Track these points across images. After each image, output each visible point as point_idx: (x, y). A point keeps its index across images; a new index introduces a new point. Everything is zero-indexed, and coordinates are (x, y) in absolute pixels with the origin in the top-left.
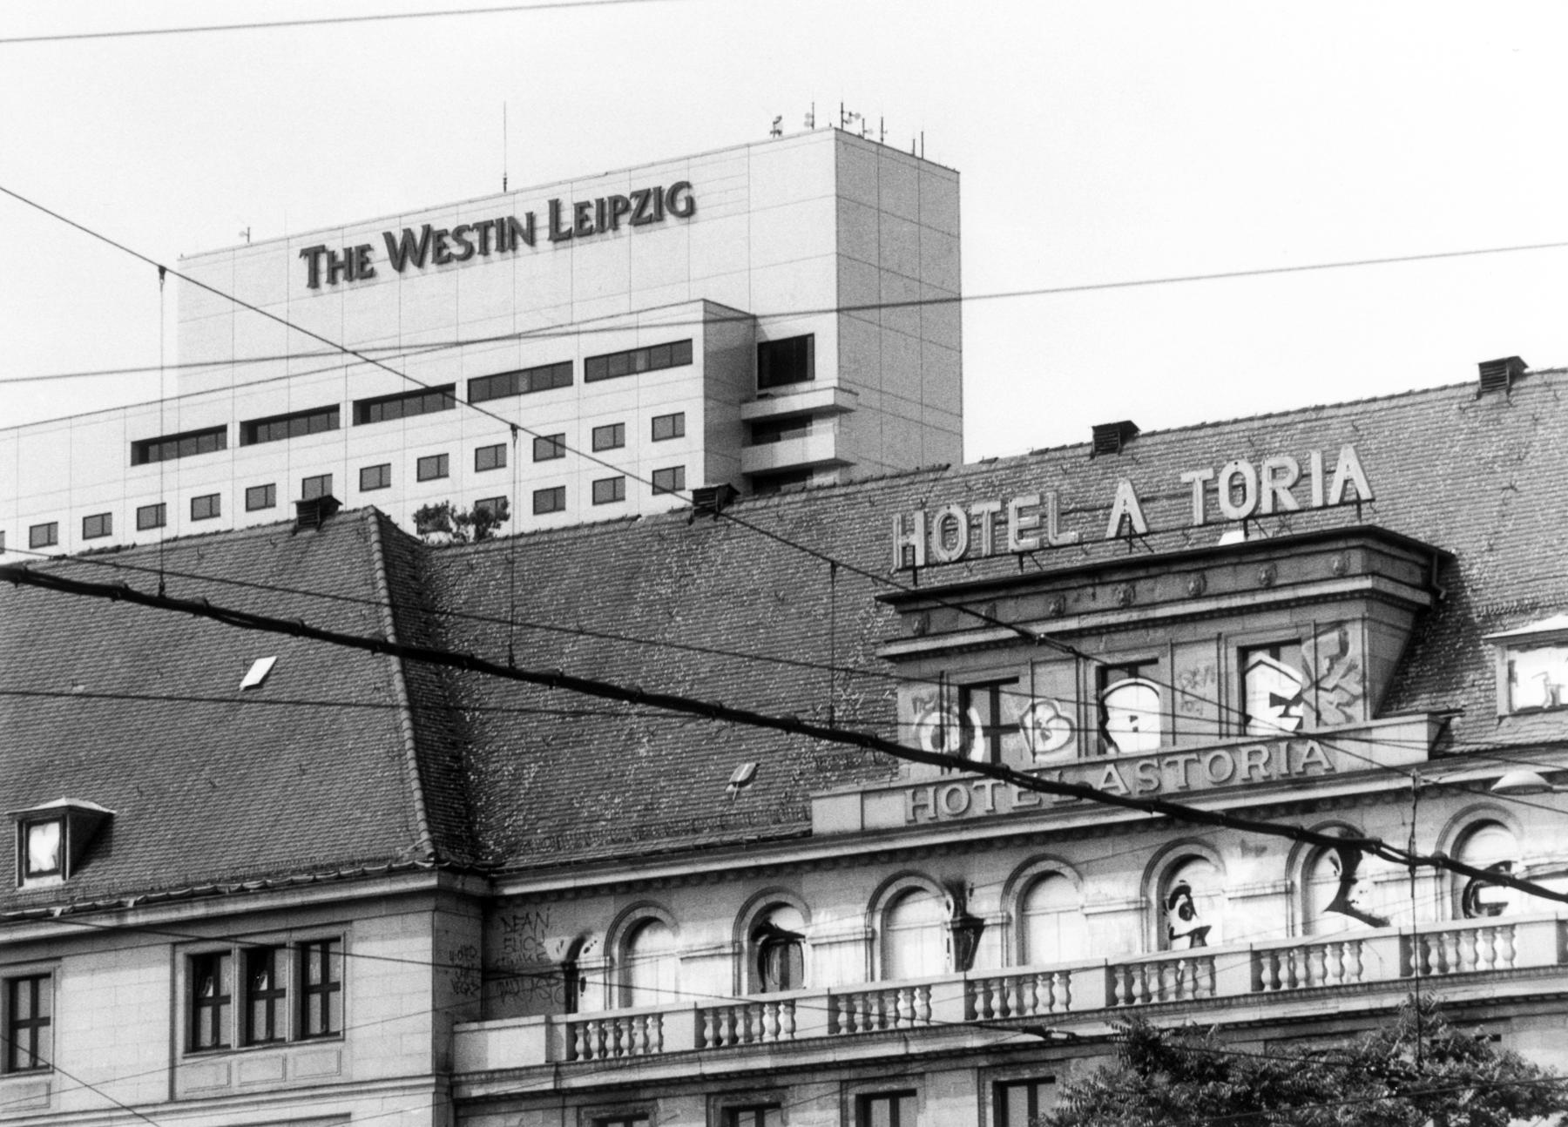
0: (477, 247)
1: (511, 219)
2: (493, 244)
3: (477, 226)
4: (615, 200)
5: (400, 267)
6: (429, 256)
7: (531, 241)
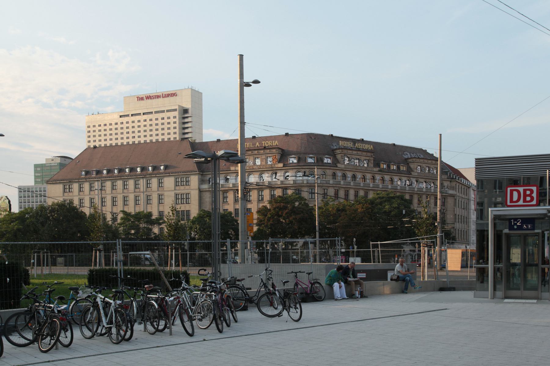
5: (147, 99)
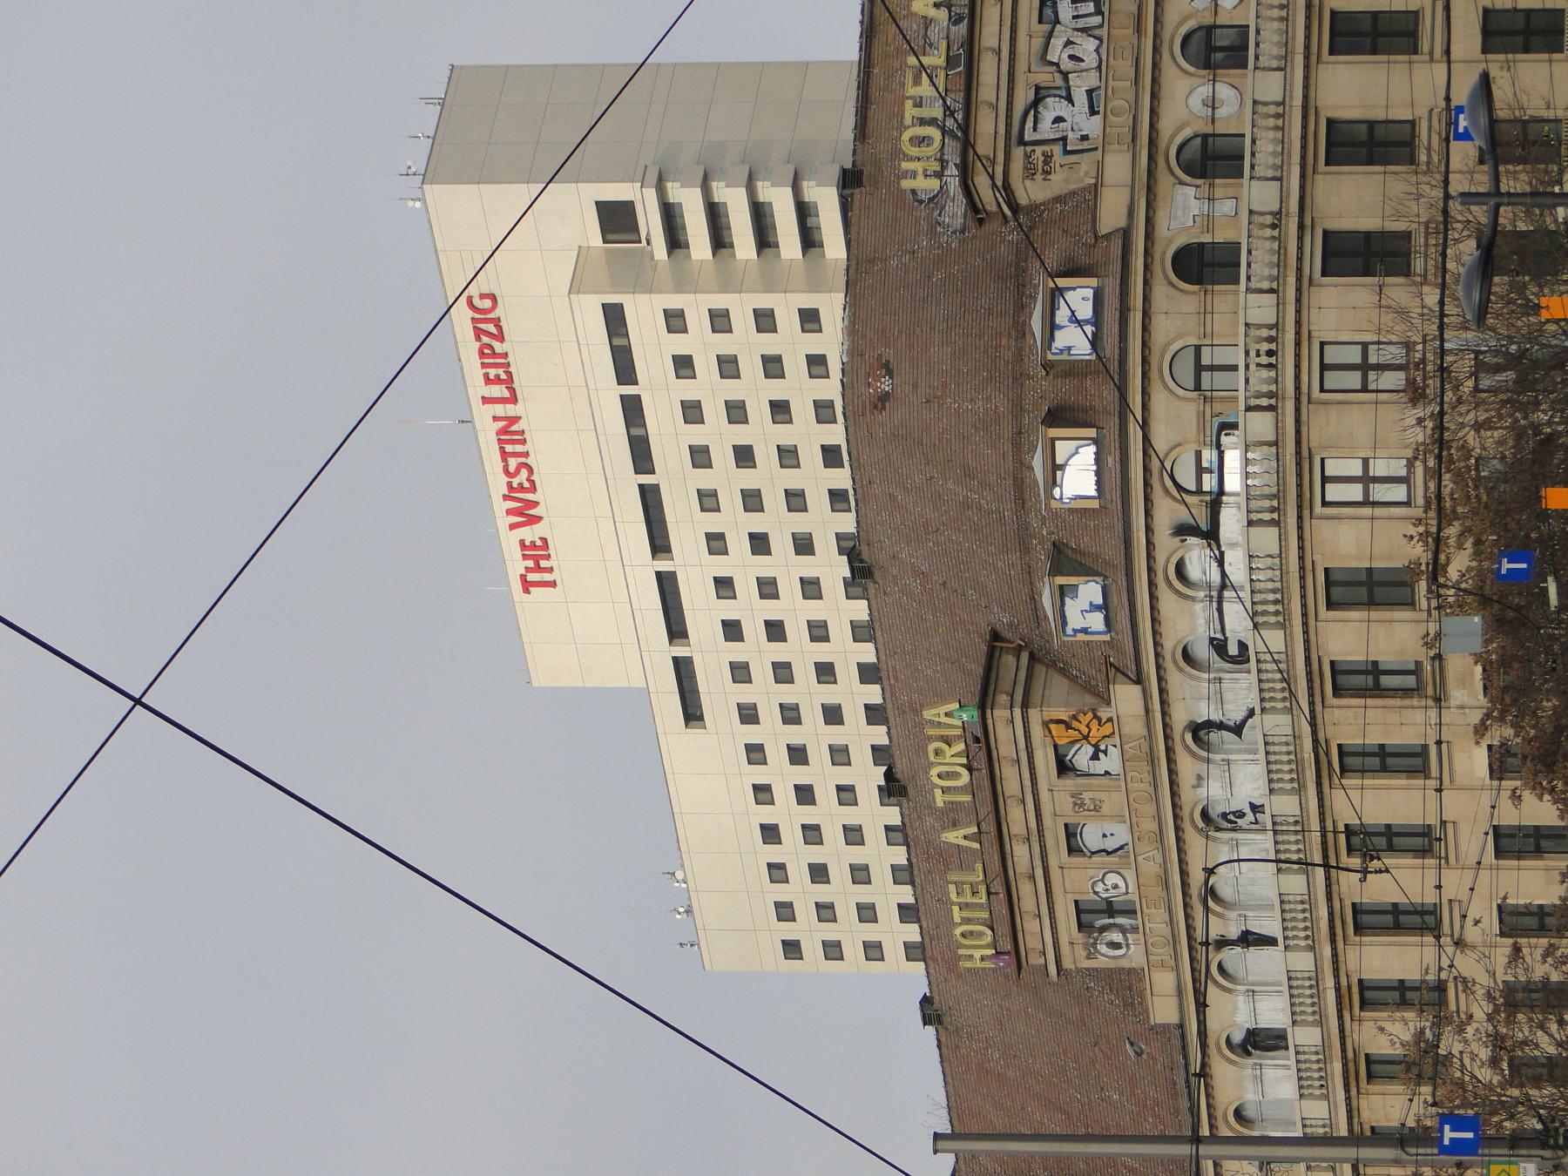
1: (498, 433)
2: (519, 448)
3: (504, 459)
4: (482, 354)
5: (537, 519)
6: (529, 496)
7: (515, 420)
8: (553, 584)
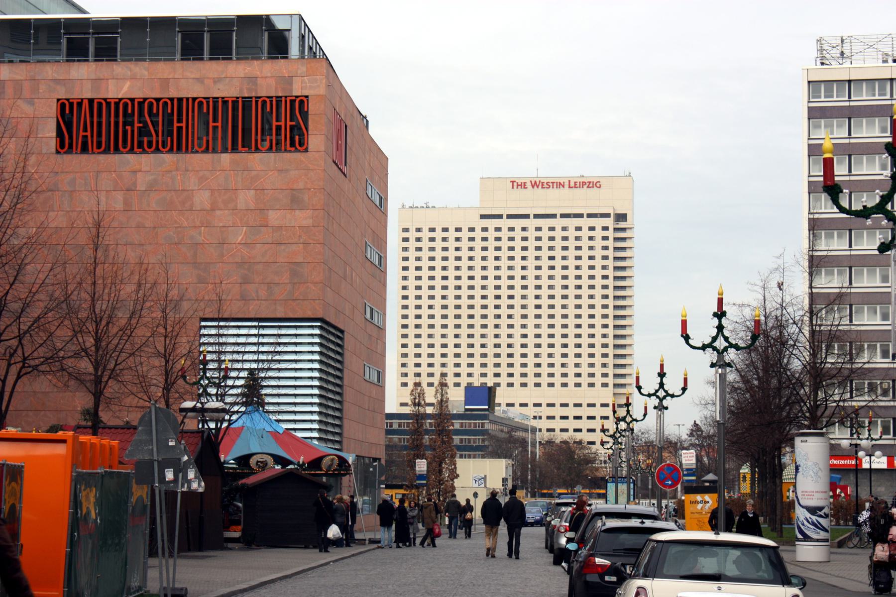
0: (551, 186)
4: (583, 182)
5: (533, 187)
6: (540, 187)
7: (563, 186)
8: (513, 188)
